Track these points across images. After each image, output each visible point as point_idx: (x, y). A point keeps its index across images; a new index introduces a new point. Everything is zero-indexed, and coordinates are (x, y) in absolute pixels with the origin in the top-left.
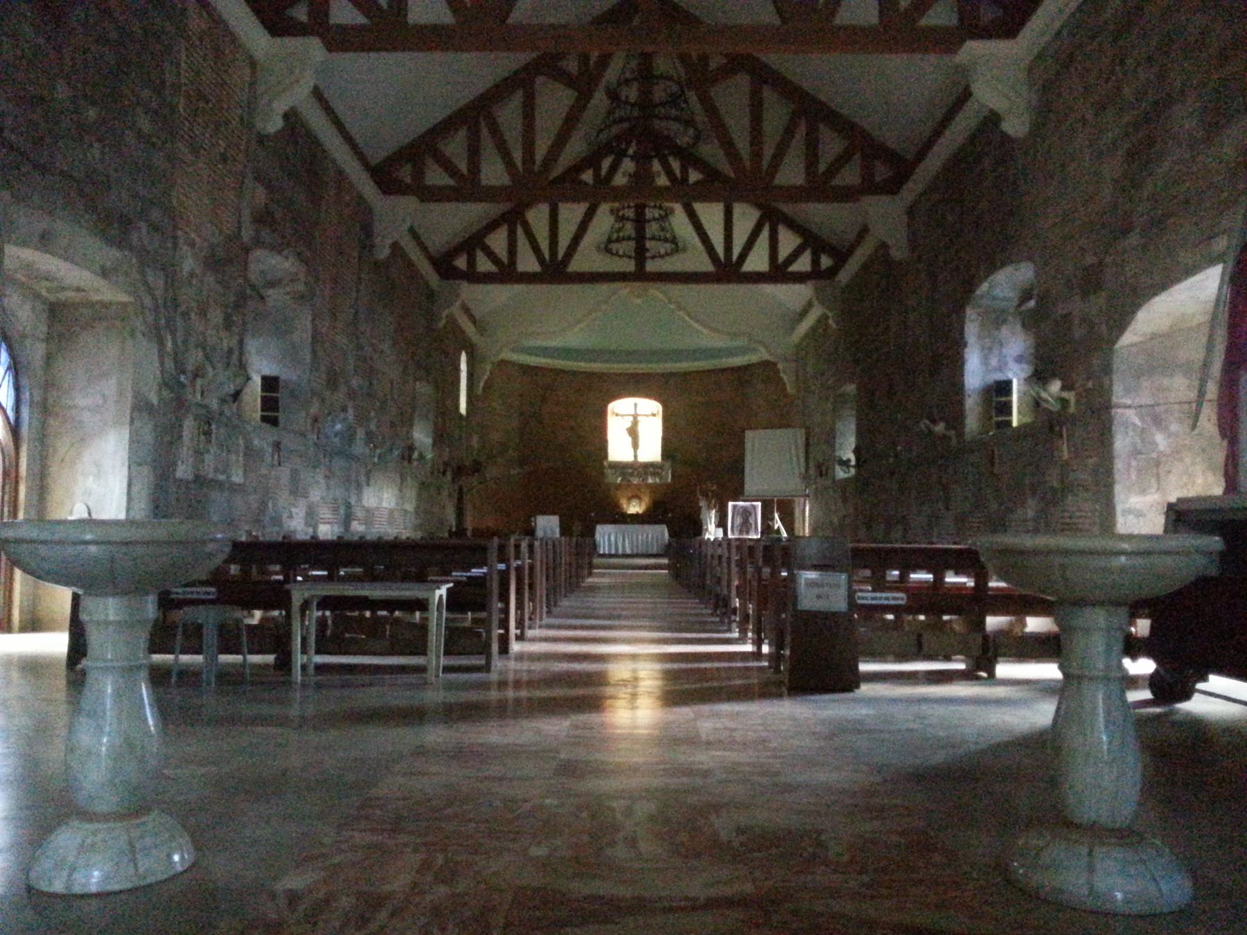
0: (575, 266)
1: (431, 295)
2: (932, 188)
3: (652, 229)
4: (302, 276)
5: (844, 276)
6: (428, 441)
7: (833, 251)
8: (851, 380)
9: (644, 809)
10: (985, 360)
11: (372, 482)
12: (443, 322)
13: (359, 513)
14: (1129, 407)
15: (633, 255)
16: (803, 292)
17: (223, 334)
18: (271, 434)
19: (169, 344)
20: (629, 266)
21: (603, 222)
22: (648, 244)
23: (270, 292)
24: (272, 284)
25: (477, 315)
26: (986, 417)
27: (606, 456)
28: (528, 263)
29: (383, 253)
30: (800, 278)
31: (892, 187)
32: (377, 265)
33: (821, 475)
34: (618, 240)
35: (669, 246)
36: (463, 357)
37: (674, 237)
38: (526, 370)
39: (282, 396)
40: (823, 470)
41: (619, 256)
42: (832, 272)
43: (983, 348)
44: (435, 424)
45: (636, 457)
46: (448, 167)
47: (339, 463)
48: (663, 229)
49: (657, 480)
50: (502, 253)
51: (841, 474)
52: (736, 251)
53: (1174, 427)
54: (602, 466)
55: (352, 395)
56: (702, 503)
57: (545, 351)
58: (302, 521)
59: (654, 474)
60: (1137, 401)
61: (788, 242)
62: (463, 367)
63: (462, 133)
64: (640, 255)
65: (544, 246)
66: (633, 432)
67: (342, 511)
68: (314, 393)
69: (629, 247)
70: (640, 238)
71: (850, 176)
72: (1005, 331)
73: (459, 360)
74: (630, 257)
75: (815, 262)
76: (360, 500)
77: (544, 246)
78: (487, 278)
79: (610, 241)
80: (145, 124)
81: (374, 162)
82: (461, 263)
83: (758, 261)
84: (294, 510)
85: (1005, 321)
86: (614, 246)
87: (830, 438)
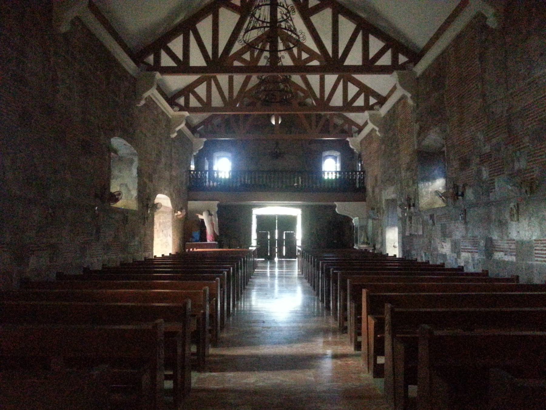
58: (450, 250)
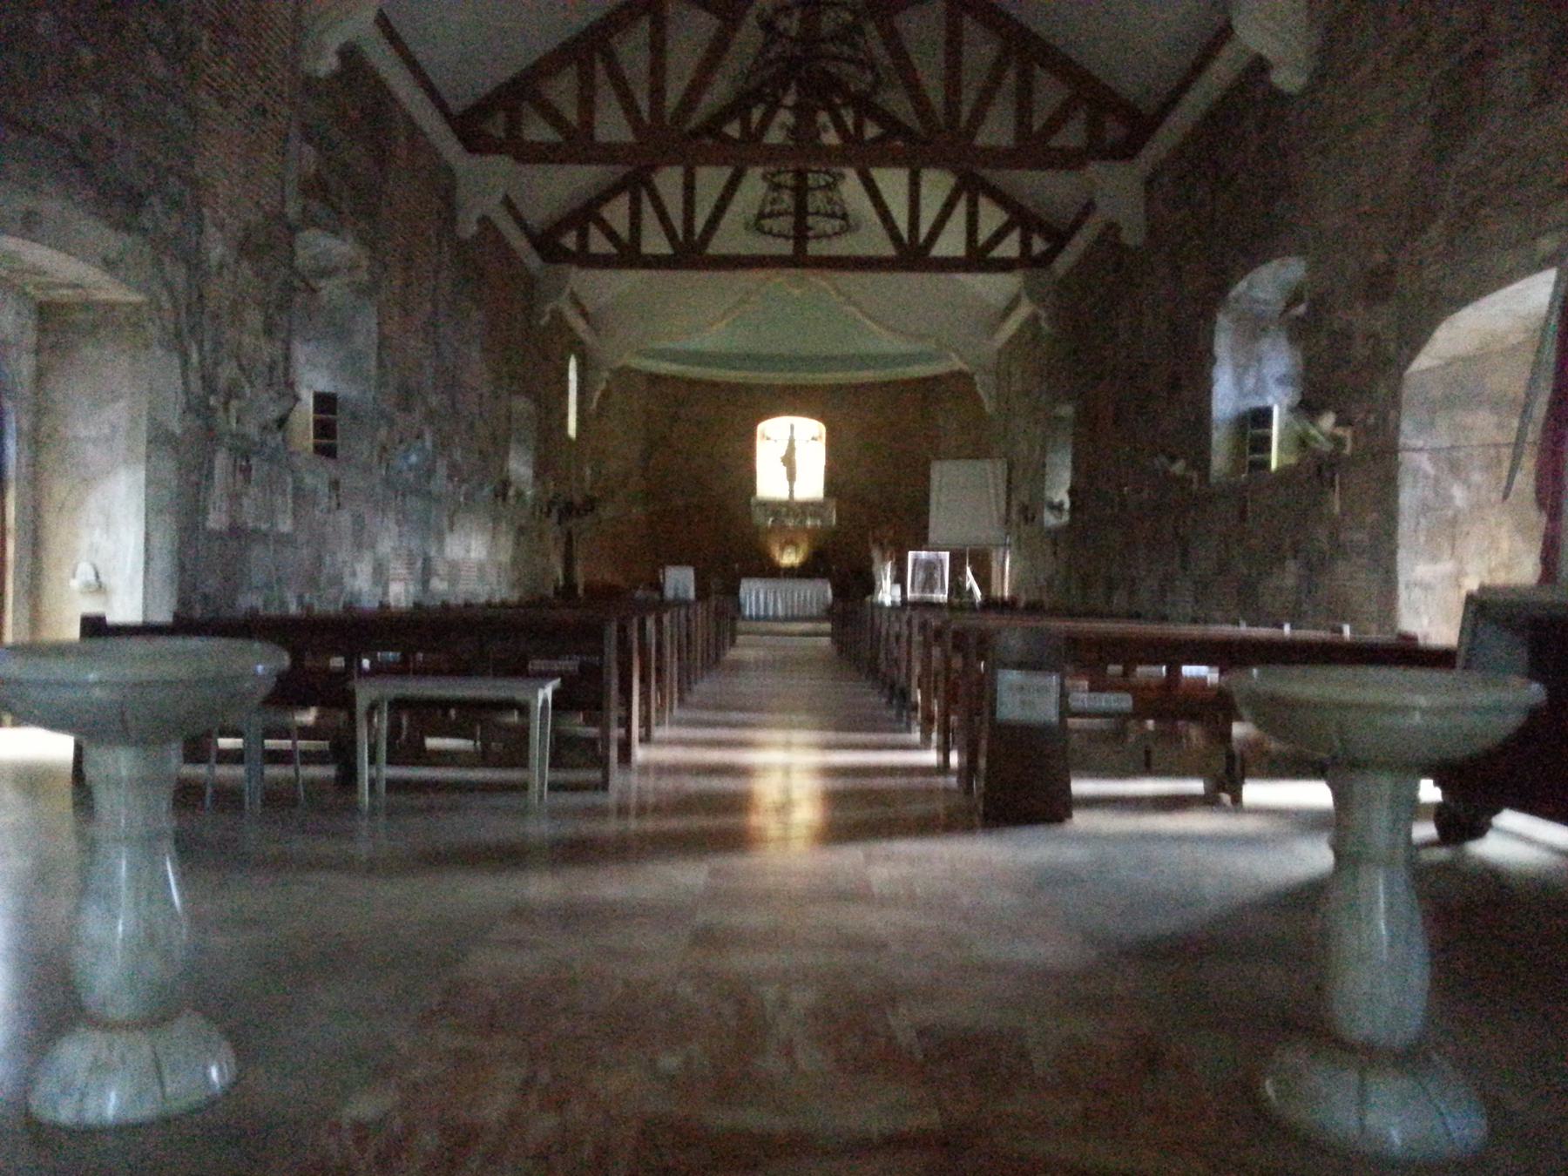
0: (717, 247)
1: (531, 282)
2: (1179, 152)
3: (816, 201)
4: (365, 263)
5: (1064, 262)
9: (804, 998)
10: (1239, 382)
11: (457, 527)
12: (547, 318)
13: (441, 568)
14: (1421, 449)
15: (792, 233)
16: (1005, 284)
17: (262, 341)
18: (329, 468)
19: (195, 357)
20: (786, 248)
21: (753, 189)
22: (810, 221)
23: (322, 283)
24: (326, 273)
25: (590, 309)
26: (1237, 453)
28: (655, 243)
29: (468, 228)
30: (1006, 266)
31: (1126, 151)
32: (460, 246)
33: (1026, 519)
34: (771, 215)
35: (837, 223)
36: (573, 365)
38: (655, 379)
39: (342, 420)
40: (1029, 514)
41: (774, 236)
43: (1236, 366)
45: (791, 492)
46: (555, 118)
47: (415, 503)
48: (830, 201)
49: (819, 523)
50: (622, 227)
51: (1050, 519)
52: (924, 229)
53: (1476, 477)
54: (749, 505)
55: (430, 416)
56: (876, 554)
57: (675, 357)
59: (815, 515)
60: (1431, 443)
61: (991, 218)
62: (573, 376)
64: (801, 234)
65: (678, 224)
66: (789, 460)
67: (419, 564)
68: (382, 415)
69: (785, 224)
70: (801, 212)
71: (1072, 135)
72: (1265, 345)
73: (567, 364)
74: (787, 237)
75: (1026, 244)
76: (441, 550)
77: (678, 224)
78: (604, 262)
79: (761, 216)
80: (157, 67)
81: (456, 107)
82: (570, 241)
83: (951, 244)
84: (358, 567)
86: (767, 223)
87: (1039, 474)
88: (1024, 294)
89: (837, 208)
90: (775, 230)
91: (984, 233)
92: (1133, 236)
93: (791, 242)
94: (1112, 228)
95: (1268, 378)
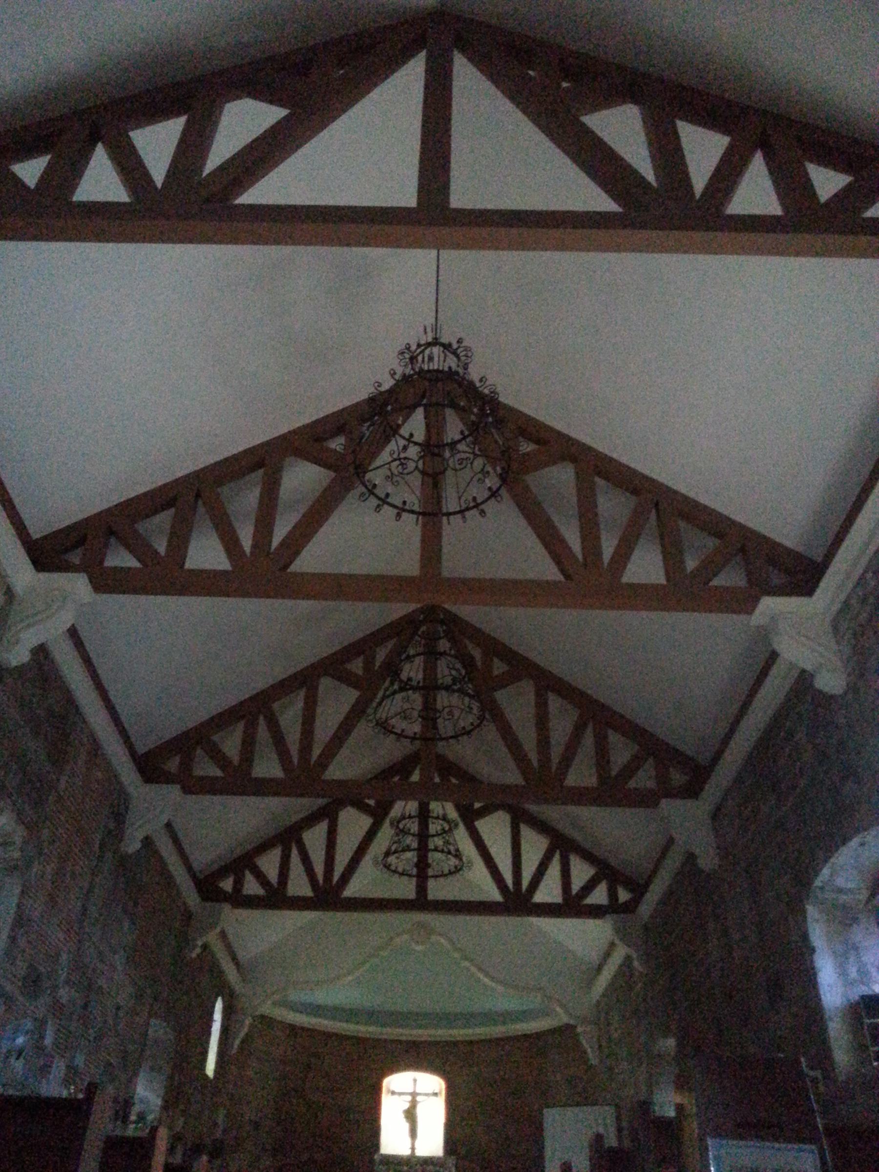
0: (351, 890)
1: (188, 916)
2: (738, 780)
6: (156, 1101)
7: (630, 884)
8: (666, 1034)
10: (843, 973)
12: (198, 950)
15: (415, 871)
20: (406, 889)
21: (385, 836)
27: (376, 1146)
29: (132, 846)
30: (596, 912)
31: (692, 791)
35: (453, 861)
36: (219, 1006)
37: (457, 850)
38: (293, 1030)
42: (629, 908)
44: (171, 1078)
45: (413, 1149)
52: (525, 883)
54: (372, 1161)
55: (57, 1008)
57: (317, 1010)
62: (218, 1016)
63: (240, 726)
66: (411, 1115)
70: (423, 850)
73: (214, 1007)
74: (410, 876)
75: (612, 894)
77: (319, 869)
78: (252, 902)
79: (388, 854)
85: (855, 920)
86: (392, 859)
88: (617, 941)
89: (452, 848)
90: (400, 870)
91: (576, 885)
92: (708, 861)
93: (415, 879)
94: (691, 857)
95: (869, 966)
